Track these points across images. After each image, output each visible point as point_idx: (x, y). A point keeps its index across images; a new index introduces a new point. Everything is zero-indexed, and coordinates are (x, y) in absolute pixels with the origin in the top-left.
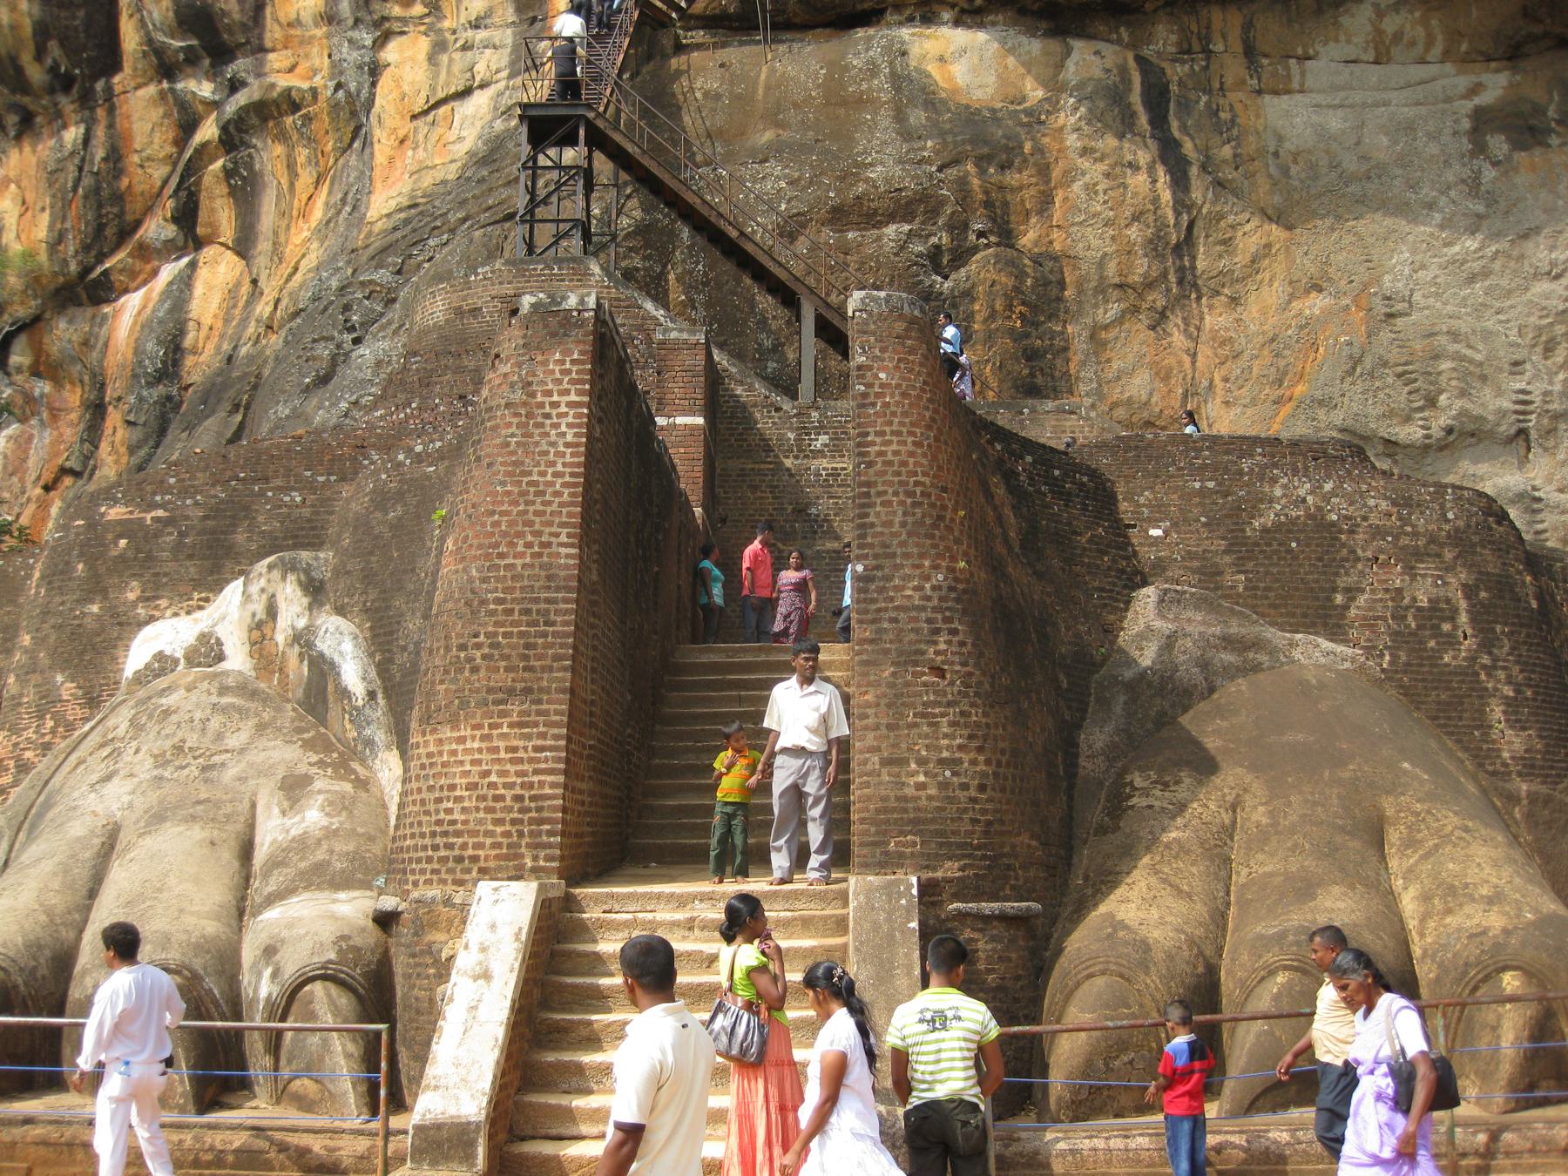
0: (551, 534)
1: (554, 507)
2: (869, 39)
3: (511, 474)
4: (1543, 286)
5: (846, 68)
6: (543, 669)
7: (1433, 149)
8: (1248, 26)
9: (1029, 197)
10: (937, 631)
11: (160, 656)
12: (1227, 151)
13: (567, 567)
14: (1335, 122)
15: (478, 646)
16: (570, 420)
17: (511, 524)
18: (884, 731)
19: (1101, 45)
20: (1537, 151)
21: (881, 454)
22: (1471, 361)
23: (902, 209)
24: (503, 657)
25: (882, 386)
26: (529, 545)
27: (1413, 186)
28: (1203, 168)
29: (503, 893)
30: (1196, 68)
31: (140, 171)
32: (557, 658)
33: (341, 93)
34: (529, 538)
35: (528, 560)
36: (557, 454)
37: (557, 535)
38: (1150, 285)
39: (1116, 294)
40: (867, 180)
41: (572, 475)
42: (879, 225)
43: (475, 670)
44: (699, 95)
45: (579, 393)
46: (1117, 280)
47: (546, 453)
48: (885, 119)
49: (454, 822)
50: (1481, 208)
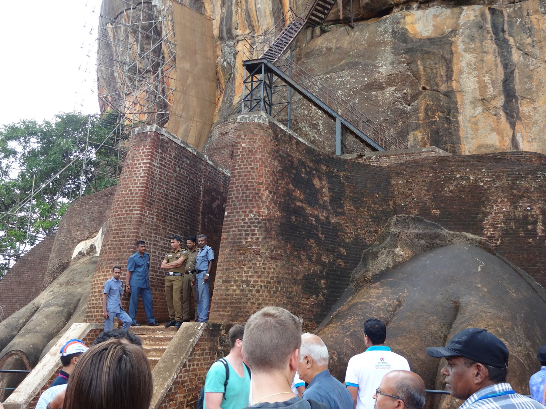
0: (133, 207)
1: (135, 198)
3: (124, 188)
6: (124, 252)
10: (247, 235)
11: (80, 253)
13: (135, 218)
15: (108, 245)
16: (143, 168)
17: (123, 204)
18: (225, 271)
21: (239, 172)
23: (391, 81)
24: (114, 248)
25: (243, 148)
26: (126, 211)
28: (518, 48)
29: (78, 327)
30: (516, 9)
31: (172, 95)
32: (129, 248)
33: (225, 63)
34: (127, 208)
35: (125, 216)
36: (139, 180)
37: (134, 207)
38: (494, 97)
39: (480, 103)
40: (379, 72)
41: (142, 187)
42: (384, 88)
43: (106, 253)
44: (324, 49)
45: (147, 159)
46: (479, 98)
47: (135, 180)
48: (389, 48)
49: (93, 304)
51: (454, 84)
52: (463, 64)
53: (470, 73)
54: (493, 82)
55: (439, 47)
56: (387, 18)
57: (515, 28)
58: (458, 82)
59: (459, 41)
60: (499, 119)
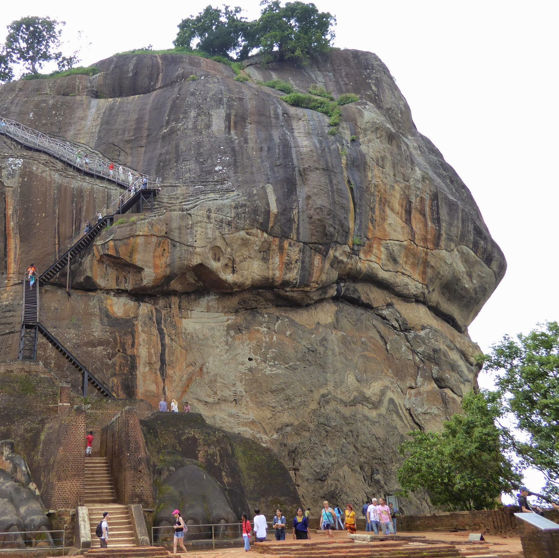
2: (94, 296)
4: (240, 367)
5: (89, 305)
7: (218, 334)
8: (180, 302)
9: (130, 342)
12: (174, 332)
14: (198, 326)
19: (147, 304)
20: (240, 334)
22: (224, 383)
27: (214, 342)
44: (53, 308)
50: (228, 348)
51: (135, 350)
52: (141, 339)
53: (144, 346)
54: (155, 353)
55: (126, 326)
56: (94, 296)
57: (167, 323)
58: (137, 350)
59: (139, 325)
60: (157, 375)
